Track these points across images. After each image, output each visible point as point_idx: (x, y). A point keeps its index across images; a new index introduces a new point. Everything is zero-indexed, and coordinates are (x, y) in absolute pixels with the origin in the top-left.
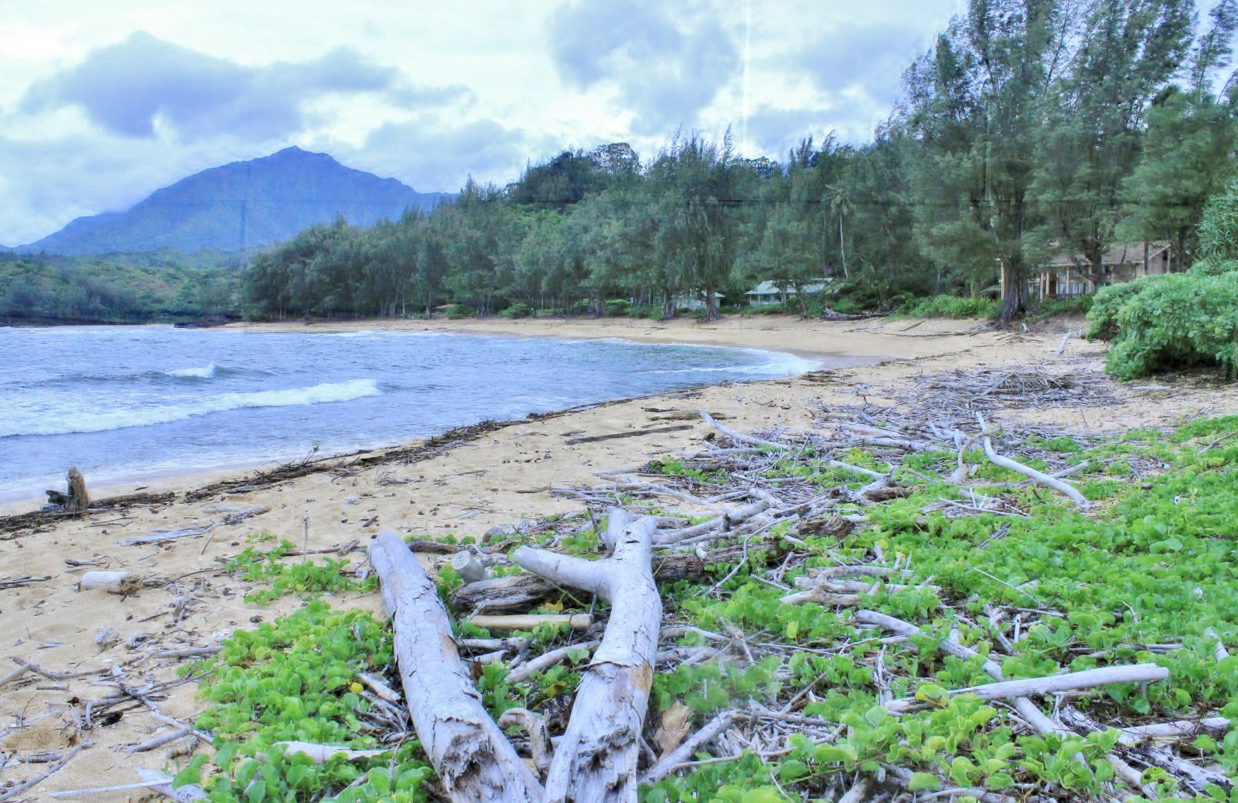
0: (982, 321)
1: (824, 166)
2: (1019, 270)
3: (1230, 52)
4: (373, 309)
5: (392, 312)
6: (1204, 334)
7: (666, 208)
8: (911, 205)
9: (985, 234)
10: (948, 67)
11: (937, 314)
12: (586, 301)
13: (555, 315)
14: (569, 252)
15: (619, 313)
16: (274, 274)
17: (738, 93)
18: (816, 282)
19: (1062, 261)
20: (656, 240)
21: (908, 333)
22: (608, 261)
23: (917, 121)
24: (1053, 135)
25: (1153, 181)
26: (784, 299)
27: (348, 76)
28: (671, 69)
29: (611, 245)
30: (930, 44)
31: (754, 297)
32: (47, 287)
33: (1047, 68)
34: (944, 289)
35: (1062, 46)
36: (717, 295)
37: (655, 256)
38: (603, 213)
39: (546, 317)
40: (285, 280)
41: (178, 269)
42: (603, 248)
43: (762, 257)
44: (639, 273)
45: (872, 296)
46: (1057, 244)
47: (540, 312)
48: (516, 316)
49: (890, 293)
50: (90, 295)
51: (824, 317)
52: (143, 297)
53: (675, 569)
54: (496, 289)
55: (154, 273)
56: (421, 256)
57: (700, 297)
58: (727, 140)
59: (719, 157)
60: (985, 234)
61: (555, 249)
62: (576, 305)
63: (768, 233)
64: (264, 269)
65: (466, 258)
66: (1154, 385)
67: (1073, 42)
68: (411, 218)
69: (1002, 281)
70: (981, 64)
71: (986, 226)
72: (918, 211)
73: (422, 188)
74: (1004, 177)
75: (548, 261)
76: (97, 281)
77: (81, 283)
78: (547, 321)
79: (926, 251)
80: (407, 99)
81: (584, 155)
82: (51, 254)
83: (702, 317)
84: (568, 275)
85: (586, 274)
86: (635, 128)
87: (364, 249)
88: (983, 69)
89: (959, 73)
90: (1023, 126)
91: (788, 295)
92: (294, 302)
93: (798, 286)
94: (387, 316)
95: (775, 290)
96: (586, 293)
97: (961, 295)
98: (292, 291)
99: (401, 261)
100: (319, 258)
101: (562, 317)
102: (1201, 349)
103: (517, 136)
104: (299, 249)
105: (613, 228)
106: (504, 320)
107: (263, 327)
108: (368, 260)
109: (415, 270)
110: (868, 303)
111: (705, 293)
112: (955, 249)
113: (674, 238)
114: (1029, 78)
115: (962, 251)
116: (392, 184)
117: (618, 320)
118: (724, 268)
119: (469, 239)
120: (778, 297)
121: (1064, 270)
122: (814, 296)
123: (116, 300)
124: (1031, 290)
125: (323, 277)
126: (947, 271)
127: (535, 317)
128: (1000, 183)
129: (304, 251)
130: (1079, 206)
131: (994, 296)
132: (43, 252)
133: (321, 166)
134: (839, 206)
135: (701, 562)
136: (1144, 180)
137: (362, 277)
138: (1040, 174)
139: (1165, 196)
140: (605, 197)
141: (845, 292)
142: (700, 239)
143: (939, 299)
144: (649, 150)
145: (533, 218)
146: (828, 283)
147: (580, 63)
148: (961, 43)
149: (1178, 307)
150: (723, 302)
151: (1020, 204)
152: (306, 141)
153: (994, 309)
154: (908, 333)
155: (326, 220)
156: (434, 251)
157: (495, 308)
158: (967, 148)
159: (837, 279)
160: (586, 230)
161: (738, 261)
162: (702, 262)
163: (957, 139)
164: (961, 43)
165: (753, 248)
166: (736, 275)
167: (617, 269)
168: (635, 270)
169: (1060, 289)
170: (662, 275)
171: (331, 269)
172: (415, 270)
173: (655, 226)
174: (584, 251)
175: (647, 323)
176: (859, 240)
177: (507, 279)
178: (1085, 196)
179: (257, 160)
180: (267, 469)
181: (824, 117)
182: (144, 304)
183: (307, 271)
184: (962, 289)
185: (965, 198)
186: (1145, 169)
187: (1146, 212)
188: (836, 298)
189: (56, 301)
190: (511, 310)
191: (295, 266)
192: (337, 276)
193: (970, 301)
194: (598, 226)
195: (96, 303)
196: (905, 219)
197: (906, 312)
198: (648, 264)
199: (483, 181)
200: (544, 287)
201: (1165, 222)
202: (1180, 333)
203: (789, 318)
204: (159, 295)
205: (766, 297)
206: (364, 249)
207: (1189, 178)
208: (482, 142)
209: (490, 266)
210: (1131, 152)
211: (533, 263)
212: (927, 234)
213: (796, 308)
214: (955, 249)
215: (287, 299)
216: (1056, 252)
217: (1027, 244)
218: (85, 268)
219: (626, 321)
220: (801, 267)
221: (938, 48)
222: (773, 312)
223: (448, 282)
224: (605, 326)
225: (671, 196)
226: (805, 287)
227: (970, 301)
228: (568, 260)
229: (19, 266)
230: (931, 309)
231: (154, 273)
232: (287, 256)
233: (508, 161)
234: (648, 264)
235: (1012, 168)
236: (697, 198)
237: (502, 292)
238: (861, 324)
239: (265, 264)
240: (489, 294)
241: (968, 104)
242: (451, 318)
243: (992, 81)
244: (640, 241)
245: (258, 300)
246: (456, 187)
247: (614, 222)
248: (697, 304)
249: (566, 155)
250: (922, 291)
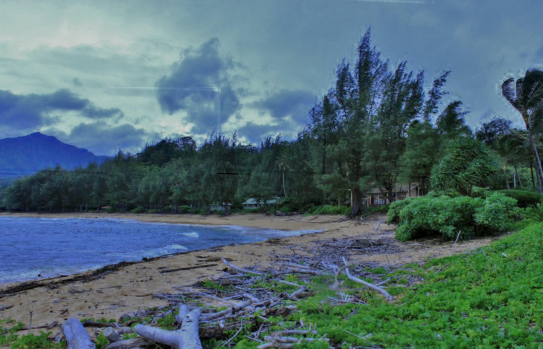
0: (343, 217)
1: (276, 149)
2: (359, 194)
3: (437, 108)
4: (72, 208)
5: (81, 210)
6: (434, 222)
7: (207, 167)
8: (313, 166)
9: (345, 179)
10: (328, 108)
11: (324, 213)
12: (170, 206)
13: (156, 212)
15: (185, 212)
17: (239, 117)
18: (272, 199)
19: (376, 191)
20: (202, 180)
21: (313, 221)
22: (181, 188)
23: (315, 131)
24: (371, 139)
25: (412, 158)
26: (258, 206)
27: (65, 102)
28: (210, 106)
29: (182, 181)
30: (320, 100)
31: (245, 205)
33: (368, 110)
34: (328, 203)
35: (374, 103)
36: (229, 204)
37: (202, 187)
38: (179, 167)
39: (153, 213)
40: (29, 193)
42: (178, 183)
43: (248, 188)
45: (296, 205)
46: (373, 183)
47: (150, 211)
49: (304, 204)
51: (276, 214)
53: (210, 333)
54: (130, 200)
56: (95, 185)
57: (222, 206)
58: (234, 137)
59: (230, 145)
60: (345, 179)
61: (157, 183)
62: (166, 208)
63: (252, 177)
65: (116, 186)
66: (416, 244)
67: (378, 101)
68: (92, 166)
69: (351, 199)
70: (341, 108)
71: (344, 176)
72: (317, 170)
73: (97, 154)
74: (351, 156)
75: (154, 188)
78: (153, 215)
79: (320, 186)
80: (92, 113)
81: (171, 141)
83: (222, 214)
84: (163, 195)
85: (171, 194)
86: (193, 130)
87: (69, 180)
88: (342, 111)
89: (333, 112)
90: (359, 135)
91: (260, 205)
93: (265, 202)
95: (255, 203)
96: (171, 202)
97: (334, 205)
99: (86, 186)
100: (46, 185)
101: (159, 213)
102: (433, 228)
103: (141, 132)
105: (183, 174)
106: (133, 214)
107: (17, 215)
108: (71, 185)
109: (92, 190)
110: (294, 209)
111: (224, 204)
112: (331, 186)
113: (210, 179)
114: (361, 115)
115: (335, 186)
116: (84, 151)
117: (185, 215)
118: (232, 192)
120: (256, 205)
121: (377, 194)
122: (272, 205)
124: (363, 203)
125: (49, 192)
126: (328, 195)
127: (147, 213)
128: (350, 158)
129: (42, 181)
130: (383, 169)
131: (349, 205)
133: (51, 142)
134: (282, 166)
135: (221, 330)
136: (408, 158)
138: (367, 154)
139: (416, 164)
140: (180, 161)
141: (286, 203)
143: (326, 207)
144: (200, 140)
145: (148, 168)
146: (278, 200)
147: (170, 102)
148: (334, 100)
149: (424, 212)
150: (232, 207)
151: (359, 167)
152: (44, 130)
153: (349, 211)
154: (313, 221)
155: (52, 166)
157: (129, 209)
158: (337, 143)
159: (282, 197)
160: (171, 174)
161: (238, 190)
162: (223, 190)
163: (332, 139)
164: (334, 100)
165: (245, 184)
166: (238, 195)
167: (184, 192)
168: (193, 193)
169: (376, 201)
170: (205, 196)
172: (92, 190)
173: (202, 174)
174: (170, 184)
175: (198, 216)
176: (291, 181)
177: (135, 196)
178: (384, 164)
179: (20, 138)
180: (14, 284)
181: (275, 129)
183: (41, 189)
184: (335, 202)
185: (335, 164)
186: (408, 153)
187: (409, 171)
188: (281, 206)
190: (136, 210)
191: (35, 187)
193: (338, 207)
194: (177, 173)
196: (310, 172)
197: (311, 213)
198: (199, 190)
199: (126, 151)
200: (151, 199)
201: (416, 175)
202: (425, 221)
203: (260, 215)
205: (251, 205)
206: (69, 180)
207: (425, 157)
208: (126, 134)
209: (127, 189)
210: (402, 146)
211: (147, 188)
212: (320, 180)
213: (265, 211)
214: (331, 186)
216: (375, 187)
217: (362, 183)
219: (189, 215)
220: (266, 193)
221: (324, 101)
222: (254, 212)
223: (108, 196)
224: (179, 217)
225: (209, 161)
226: (267, 201)
227: (338, 207)
228: (162, 188)
230: (322, 211)
232: (32, 182)
233: (137, 143)
234: (199, 190)
235: (354, 152)
236: (221, 162)
237: (132, 202)
238: (292, 217)
240: (126, 202)
241: (337, 124)
242: (109, 213)
243: (345, 115)
244: (195, 179)
246: (113, 153)
247: (184, 171)
248: (220, 208)
249: (163, 141)
250: (318, 203)
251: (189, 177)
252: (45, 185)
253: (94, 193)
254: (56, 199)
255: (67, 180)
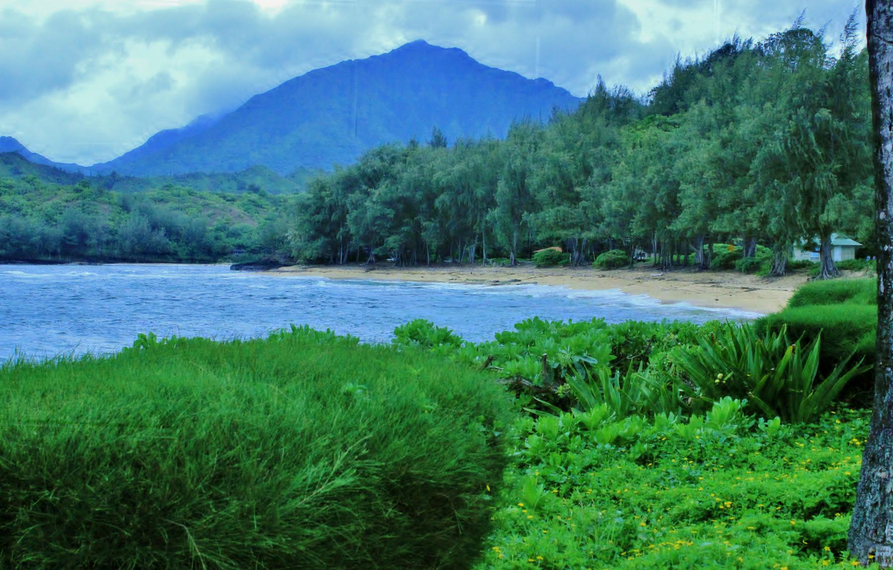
14: (664, 182)
16: (332, 209)
32: (104, 218)
41: (263, 195)
44: (737, 212)
48: (610, 265)
50: (154, 227)
52: (217, 229)
55: (233, 200)
64: (322, 198)
76: (162, 211)
77: (144, 212)
82: (122, 175)
92: (356, 243)
94: (456, 264)
98: (353, 230)
99: (480, 192)
104: (364, 175)
119: (557, 165)
123: (184, 232)
129: (373, 179)
132: (114, 174)
137: (432, 213)
142: (808, 167)
156: (519, 179)
171: (401, 200)
172: (492, 204)
182: (217, 238)
189: (112, 232)
190: (602, 257)
191: (355, 196)
192: (405, 209)
195: (159, 237)
204: (237, 226)
215: (348, 237)
218: (152, 192)
229: (77, 191)
231: (233, 200)
232: (349, 184)
239: (323, 193)
242: (539, 267)
245: (313, 238)
251: (721, 160)
252: (377, 192)
253: (496, 212)
254: (405, 228)
255: (431, 176)
